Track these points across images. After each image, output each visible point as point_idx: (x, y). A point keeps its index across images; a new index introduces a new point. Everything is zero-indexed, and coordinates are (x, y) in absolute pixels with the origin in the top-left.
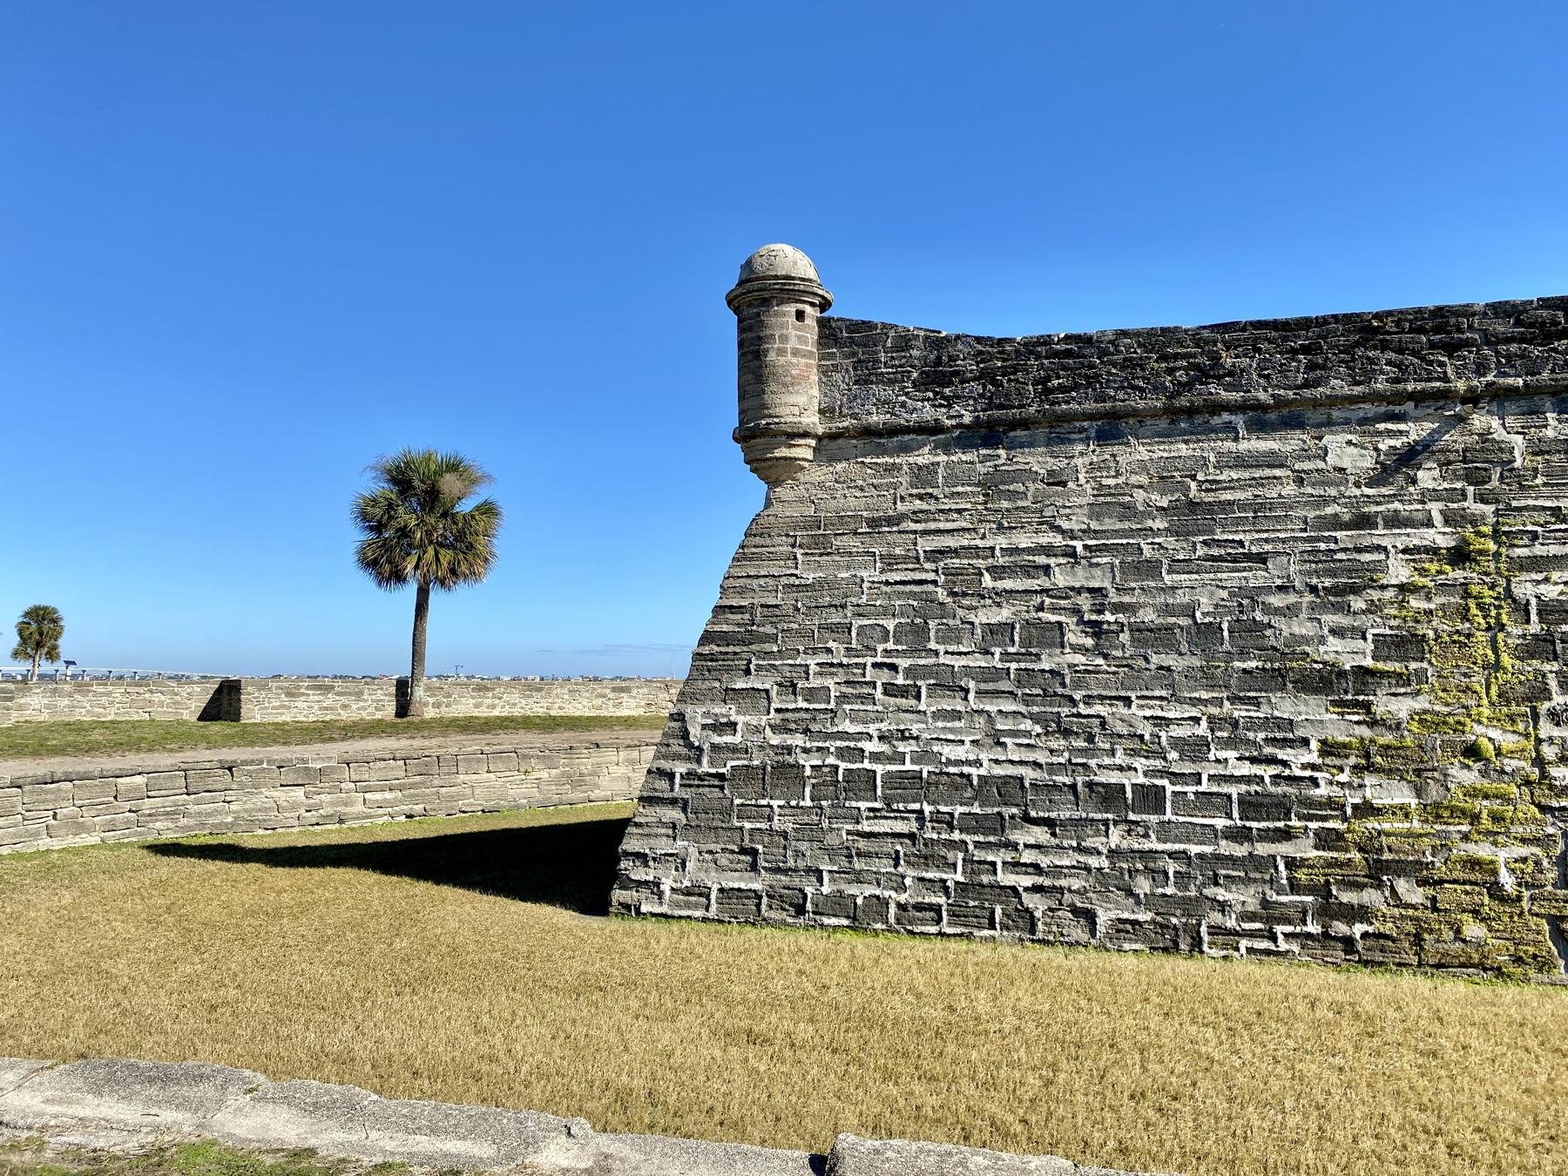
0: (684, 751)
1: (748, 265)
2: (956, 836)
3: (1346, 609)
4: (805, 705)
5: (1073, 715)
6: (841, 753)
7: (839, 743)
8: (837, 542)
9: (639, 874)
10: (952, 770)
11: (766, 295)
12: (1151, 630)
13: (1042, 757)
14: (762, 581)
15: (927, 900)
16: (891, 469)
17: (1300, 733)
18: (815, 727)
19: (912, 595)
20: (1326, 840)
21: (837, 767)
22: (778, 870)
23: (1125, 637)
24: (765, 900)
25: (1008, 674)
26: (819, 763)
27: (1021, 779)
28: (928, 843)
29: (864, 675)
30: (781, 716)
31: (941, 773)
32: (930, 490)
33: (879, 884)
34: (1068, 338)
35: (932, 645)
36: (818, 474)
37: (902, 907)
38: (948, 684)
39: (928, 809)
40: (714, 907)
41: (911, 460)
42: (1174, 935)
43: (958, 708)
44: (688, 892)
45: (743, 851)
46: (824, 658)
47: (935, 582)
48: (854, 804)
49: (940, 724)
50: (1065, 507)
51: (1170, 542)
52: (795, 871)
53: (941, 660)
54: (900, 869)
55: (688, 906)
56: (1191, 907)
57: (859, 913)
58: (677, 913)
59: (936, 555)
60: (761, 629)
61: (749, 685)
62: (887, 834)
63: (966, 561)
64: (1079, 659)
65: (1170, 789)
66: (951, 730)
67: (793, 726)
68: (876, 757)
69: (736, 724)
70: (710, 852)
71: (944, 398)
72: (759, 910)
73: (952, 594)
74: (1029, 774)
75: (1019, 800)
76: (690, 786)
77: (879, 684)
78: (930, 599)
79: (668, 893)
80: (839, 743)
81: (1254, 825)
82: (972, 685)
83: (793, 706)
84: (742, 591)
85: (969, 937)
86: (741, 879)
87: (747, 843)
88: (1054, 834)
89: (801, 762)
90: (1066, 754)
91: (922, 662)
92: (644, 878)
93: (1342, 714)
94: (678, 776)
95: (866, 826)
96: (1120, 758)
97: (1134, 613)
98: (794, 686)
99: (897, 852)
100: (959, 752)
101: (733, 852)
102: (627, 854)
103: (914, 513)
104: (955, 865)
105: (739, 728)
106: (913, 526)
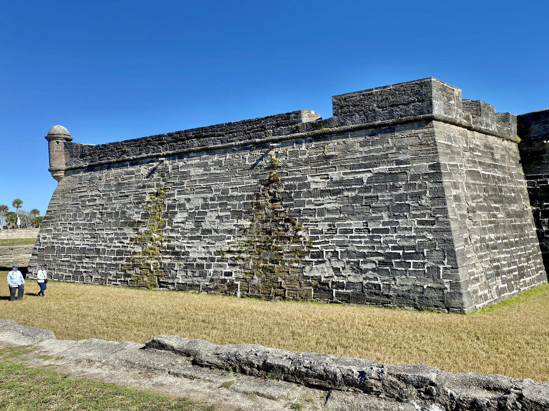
3: (138, 207)
13: (89, 243)
20: (128, 260)
36: (65, 179)
42: (102, 282)
56: (106, 275)
82: (82, 227)
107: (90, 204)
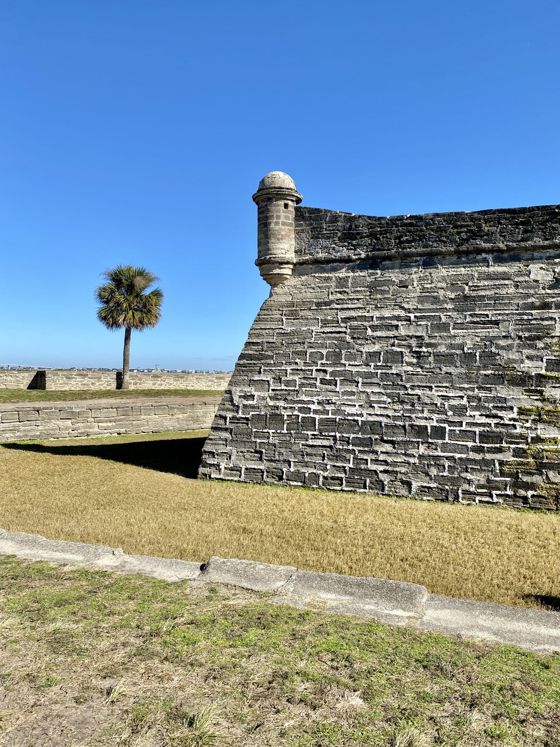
0: (231, 407)
1: (263, 182)
2: (351, 447)
4: (285, 388)
5: (406, 394)
6: (301, 410)
7: (300, 405)
8: (301, 313)
9: (210, 461)
10: (350, 418)
11: (270, 196)
12: (443, 356)
13: (390, 413)
14: (267, 331)
15: (336, 475)
16: (328, 279)
17: (509, 404)
18: (289, 398)
19: (335, 338)
20: (518, 453)
21: (298, 416)
22: (271, 461)
23: (431, 359)
24: (265, 473)
25: (377, 375)
26: (291, 414)
27: (381, 422)
28: (338, 450)
29: (312, 375)
30: (274, 392)
31: (345, 419)
32: (345, 289)
33: (315, 468)
34: (411, 217)
35: (343, 361)
36: (292, 281)
37: (325, 478)
38: (350, 379)
39: (338, 435)
40: (243, 476)
41: (337, 275)
43: (354, 390)
44: (232, 469)
45: (256, 452)
46: (294, 367)
47: (345, 333)
48: (306, 432)
49: (345, 397)
50: (406, 298)
51: (454, 314)
52: (279, 461)
53: (347, 369)
54: (325, 461)
55: (232, 475)
56: (455, 481)
57: (307, 480)
58: (227, 478)
59: (346, 320)
60: (266, 353)
61: (260, 379)
62: (320, 446)
63: (360, 323)
64: (410, 368)
65: (448, 428)
66: (350, 400)
67: (279, 397)
68: (316, 412)
70: (242, 452)
71: (352, 245)
72: (263, 478)
73: (353, 338)
74: (384, 420)
75: (379, 432)
76: (234, 423)
77: (318, 379)
78: (343, 340)
79: (223, 469)
80: (300, 405)
81: (486, 445)
82: (360, 380)
83: (279, 388)
84: (258, 336)
85: (354, 492)
86: (255, 464)
87: (258, 449)
88: (394, 448)
89: (283, 413)
90: (402, 412)
91: (338, 369)
92: (213, 462)
93: (529, 396)
94: (228, 418)
95: (310, 442)
96: (426, 414)
97: (436, 347)
98: (280, 379)
99: (324, 454)
100: (353, 410)
101: (252, 452)
102: (205, 452)
103: (337, 300)
104: (349, 460)
105: (255, 397)
106: (337, 306)
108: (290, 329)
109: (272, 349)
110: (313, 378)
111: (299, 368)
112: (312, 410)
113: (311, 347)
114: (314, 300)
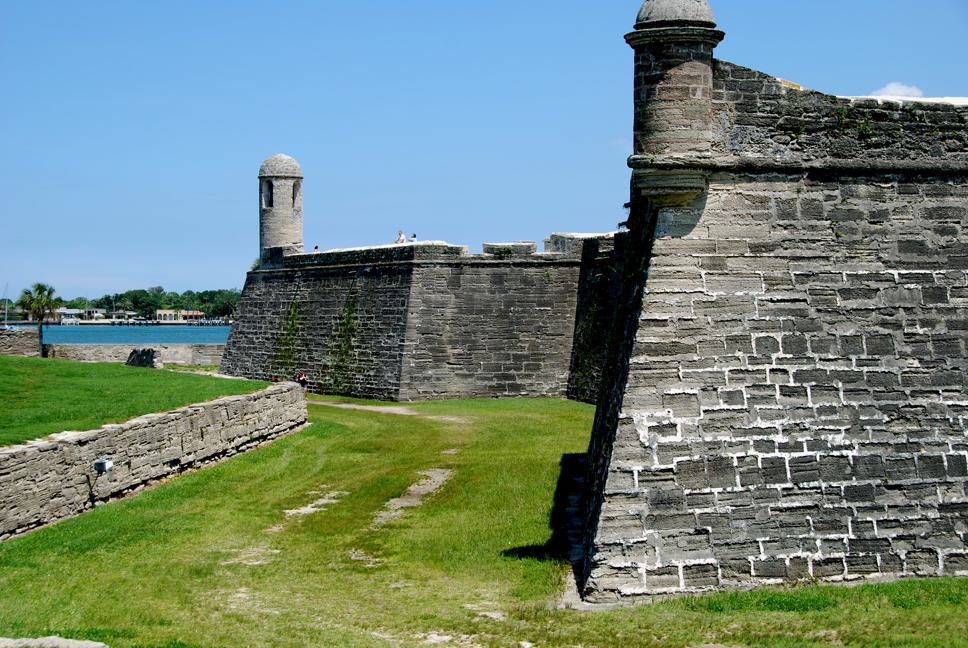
2: (845, 504)
4: (726, 407)
5: (906, 406)
6: (758, 445)
7: (756, 437)
10: (836, 453)
12: (945, 340)
14: (677, 298)
15: (832, 556)
19: (791, 312)
21: (756, 457)
23: (930, 346)
24: (720, 571)
26: (743, 454)
28: (827, 512)
29: (765, 379)
32: (793, 222)
35: (810, 354)
37: (816, 564)
38: (824, 385)
43: (834, 404)
44: (660, 572)
48: (773, 486)
49: (823, 418)
50: (883, 242)
53: (818, 366)
66: (832, 422)
67: (719, 425)
68: (783, 447)
69: (675, 425)
77: (777, 387)
78: (802, 314)
80: (756, 437)
83: (716, 408)
90: (905, 436)
91: (805, 368)
92: (623, 565)
94: (636, 474)
96: (937, 437)
97: (933, 327)
99: (808, 521)
104: (846, 526)
105: (679, 428)
107: (852, 304)
108: (715, 294)
109: (692, 332)
110: (768, 386)
111: (743, 368)
112: (777, 444)
113: (757, 329)
114: (748, 240)
